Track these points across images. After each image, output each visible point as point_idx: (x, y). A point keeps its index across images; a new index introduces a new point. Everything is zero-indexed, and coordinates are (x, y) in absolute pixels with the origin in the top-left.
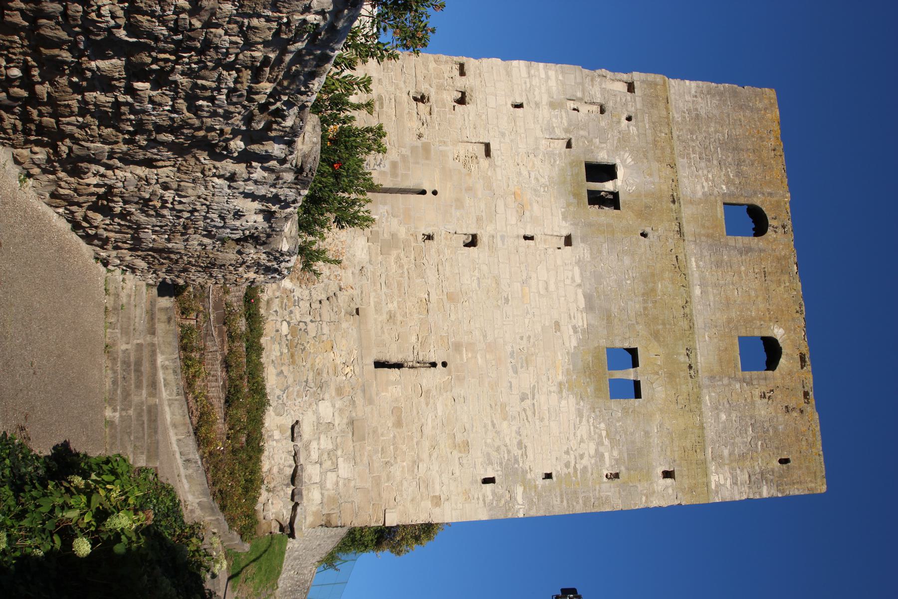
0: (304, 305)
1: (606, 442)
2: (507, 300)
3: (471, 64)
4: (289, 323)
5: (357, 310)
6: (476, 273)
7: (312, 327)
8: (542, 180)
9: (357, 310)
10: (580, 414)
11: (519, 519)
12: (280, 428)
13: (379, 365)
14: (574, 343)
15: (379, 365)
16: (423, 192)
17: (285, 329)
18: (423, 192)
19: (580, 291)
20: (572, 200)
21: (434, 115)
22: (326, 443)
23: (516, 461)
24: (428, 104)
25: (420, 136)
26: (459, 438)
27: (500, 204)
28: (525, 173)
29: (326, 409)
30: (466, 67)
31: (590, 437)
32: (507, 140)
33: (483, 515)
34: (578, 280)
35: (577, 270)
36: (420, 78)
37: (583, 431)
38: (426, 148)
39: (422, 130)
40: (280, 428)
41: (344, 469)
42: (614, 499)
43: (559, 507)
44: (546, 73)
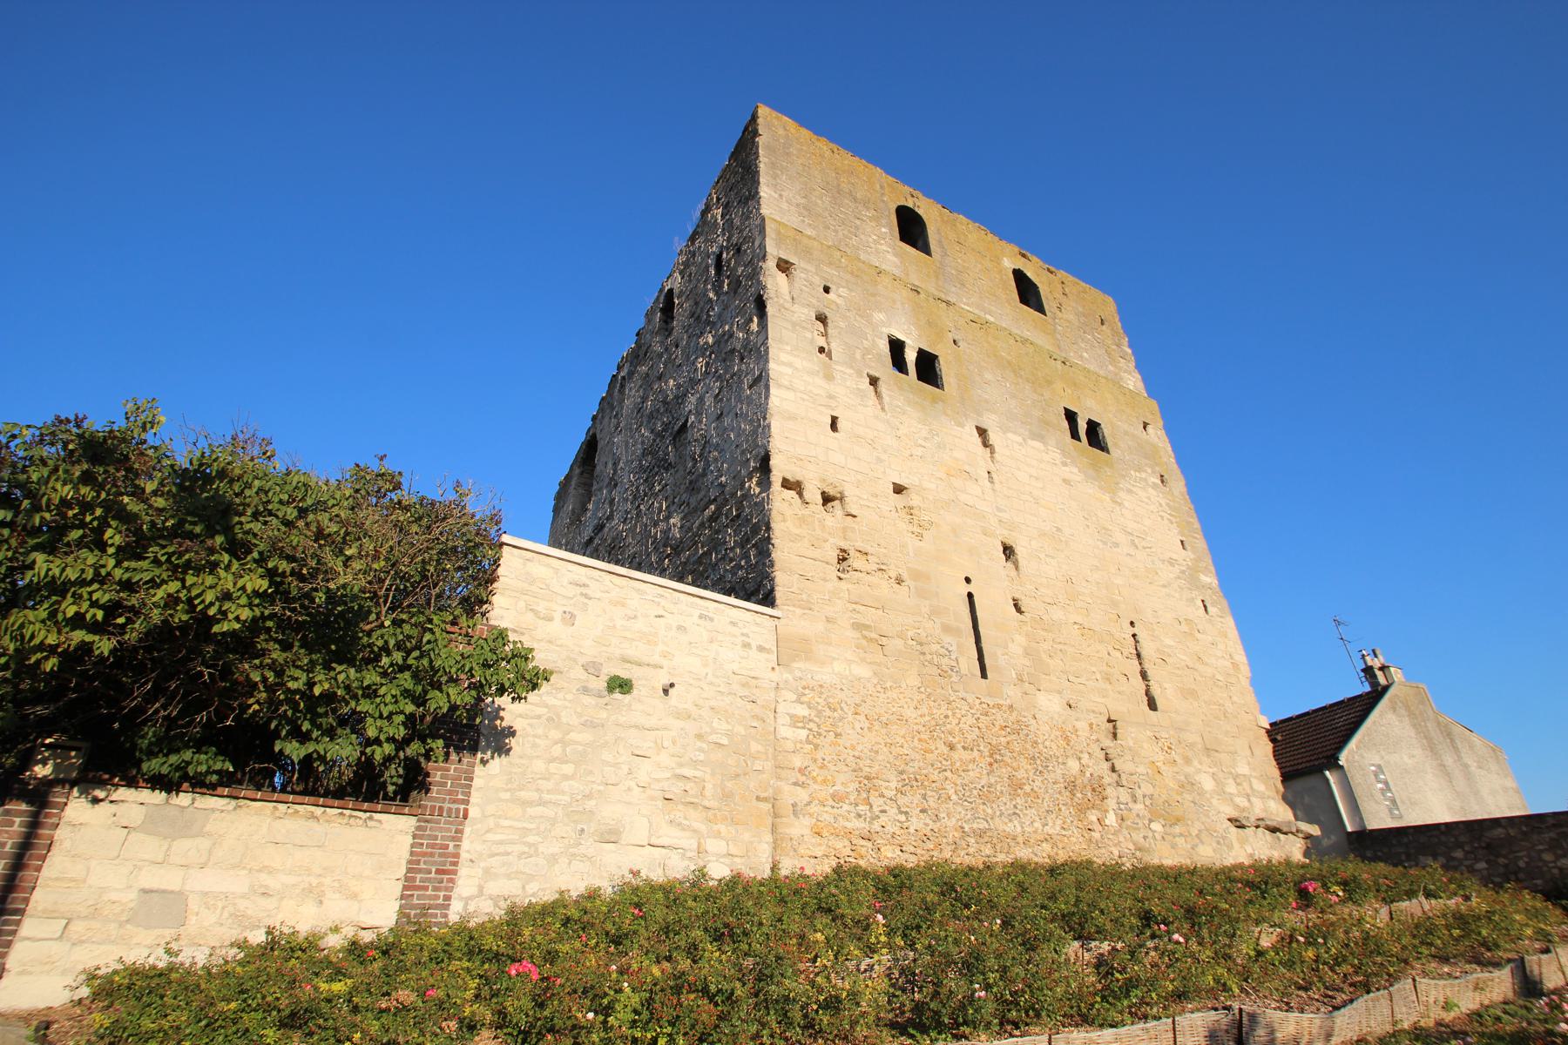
0: (1124, 795)
1: (1144, 475)
2: (1058, 529)
3: (780, 467)
4: (1151, 821)
5: (1110, 721)
6: (1042, 556)
7: (1146, 789)
8: (924, 433)
9: (1110, 721)
10: (1130, 491)
11: (1221, 585)
12: (1242, 842)
13: (1152, 705)
14: (1075, 470)
15: (1152, 705)
16: (970, 595)
17: (1156, 826)
18: (970, 595)
19: (1030, 442)
20: (940, 406)
21: (868, 549)
22: (1231, 788)
23: (1183, 572)
24: (852, 553)
25: (899, 581)
26: (1184, 628)
27: (963, 497)
28: (918, 452)
29: (1208, 784)
30: (789, 477)
31: (1144, 489)
32: (884, 457)
33: (1230, 622)
34: (1019, 439)
35: (1010, 435)
36: (817, 554)
37: (1140, 493)
38: (917, 575)
39: (893, 575)
40: (1242, 842)
41: (1243, 769)
42: (1178, 485)
43: (1201, 544)
44: (783, 364)
